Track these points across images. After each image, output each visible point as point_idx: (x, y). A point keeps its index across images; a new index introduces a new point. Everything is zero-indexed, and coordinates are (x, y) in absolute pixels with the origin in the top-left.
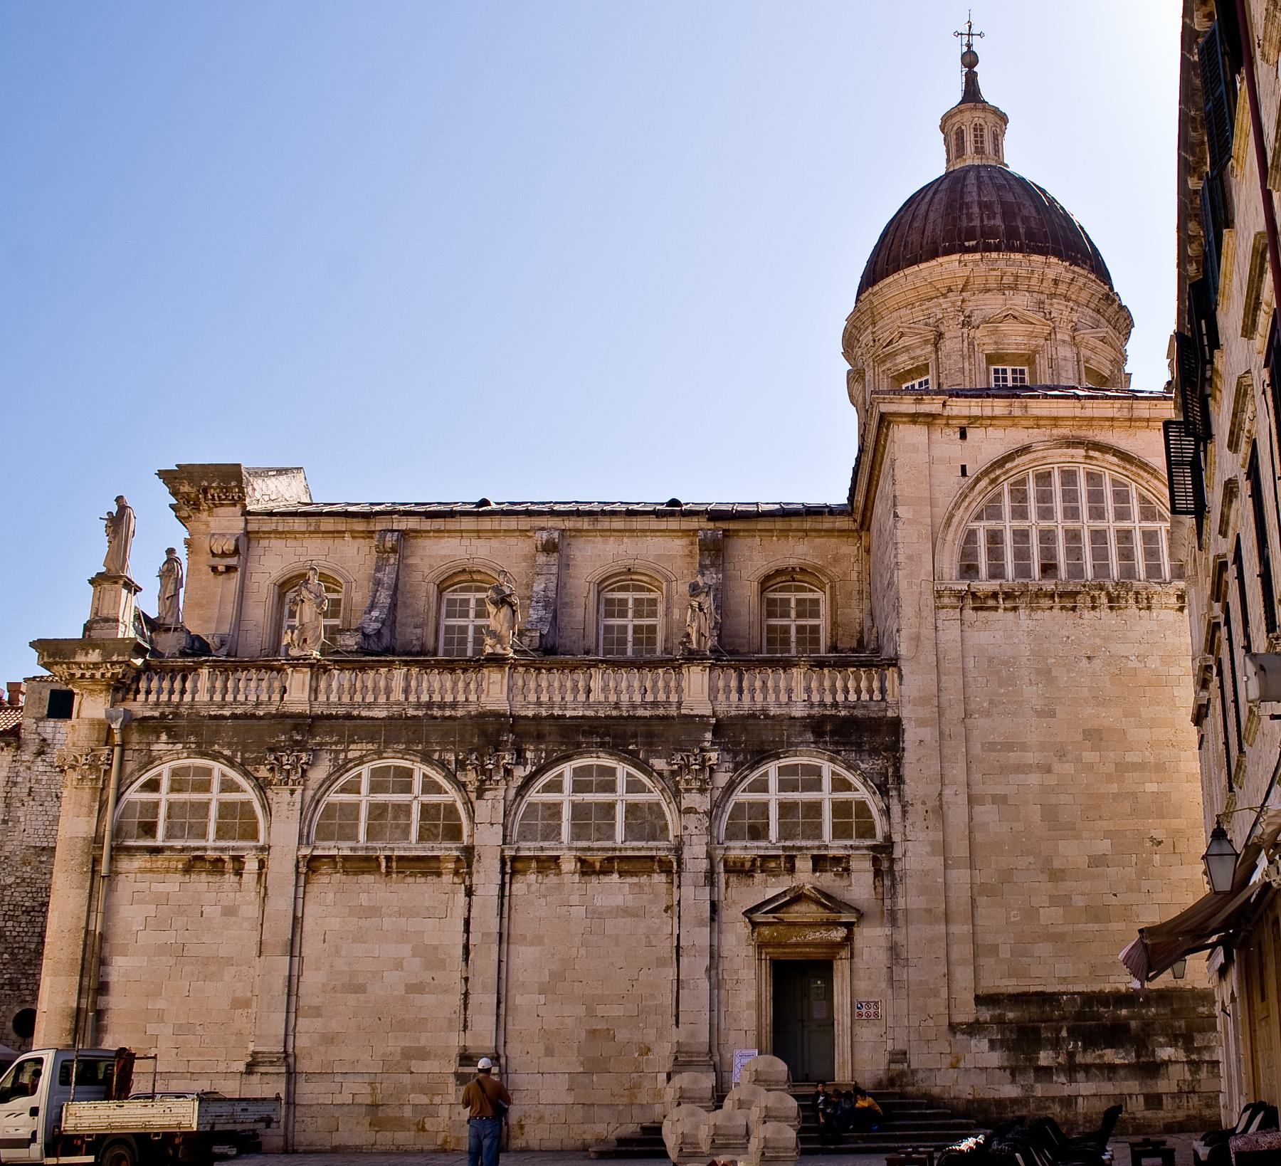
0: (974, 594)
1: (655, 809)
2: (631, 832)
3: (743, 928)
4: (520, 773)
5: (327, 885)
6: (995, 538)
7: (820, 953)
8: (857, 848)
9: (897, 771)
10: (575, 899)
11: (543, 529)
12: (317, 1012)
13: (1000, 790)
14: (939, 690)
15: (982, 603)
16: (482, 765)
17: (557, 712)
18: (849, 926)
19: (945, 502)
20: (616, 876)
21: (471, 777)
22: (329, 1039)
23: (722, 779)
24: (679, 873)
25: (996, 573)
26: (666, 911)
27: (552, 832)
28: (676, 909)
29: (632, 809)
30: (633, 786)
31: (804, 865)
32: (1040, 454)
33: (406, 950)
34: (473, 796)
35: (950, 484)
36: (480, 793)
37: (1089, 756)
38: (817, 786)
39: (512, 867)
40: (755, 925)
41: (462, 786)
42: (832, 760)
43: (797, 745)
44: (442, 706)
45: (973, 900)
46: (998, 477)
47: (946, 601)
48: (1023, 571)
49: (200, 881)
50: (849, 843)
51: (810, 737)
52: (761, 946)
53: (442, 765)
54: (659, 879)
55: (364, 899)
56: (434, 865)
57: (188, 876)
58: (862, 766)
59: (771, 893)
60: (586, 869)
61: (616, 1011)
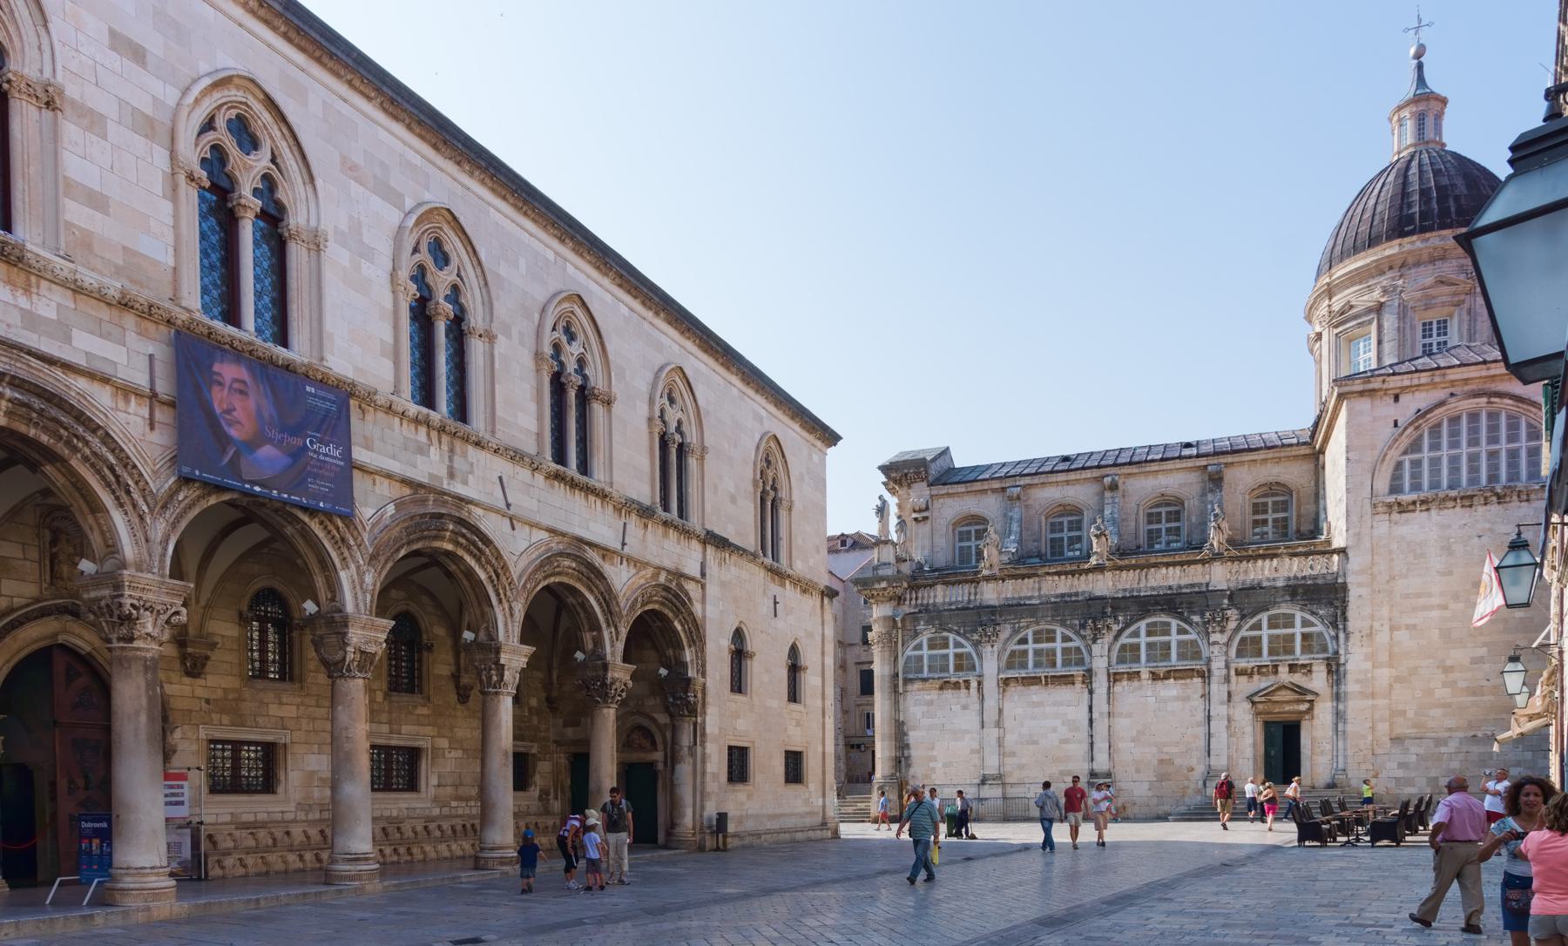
0: (1399, 504)
1: (1194, 643)
2: (1181, 656)
3: (1248, 706)
4: (1116, 628)
5: (1015, 691)
7: (1293, 717)
8: (1317, 659)
9: (1344, 613)
10: (1149, 693)
11: (1108, 476)
12: (1013, 754)
13: (1412, 621)
14: (1373, 564)
15: (1403, 508)
16: (1095, 625)
17: (1135, 594)
18: (1311, 702)
20: (1172, 680)
21: (1088, 632)
22: (1021, 767)
23: (1232, 625)
24: (1209, 677)
26: (1202, 696)
27: (1137, 659)
30: (1181, 631)
31: (1283, 670)
32: (1453, 405)
33: (1058, 723)
34: (1090, 642)
36: (1094, 641)
39: (1114, 678)
40: (1253, 703)
41: (1084, 637)
42: (1302, 610)
43: (1279, 603)
44: (1070, 595)
45: (1391, 686)
46: (1420, 425)
47: (1380, 509)
48: (1435, 485)
50: (1313, 656)
51: (1288, 598)
52: (1258, 714)
53: (1072, 627)
54: (1200, 680)
55: (1035, 698)
56: (1071, 679)
58: (1321, 612)
59: (1263, 685)
60: (1155, 677)
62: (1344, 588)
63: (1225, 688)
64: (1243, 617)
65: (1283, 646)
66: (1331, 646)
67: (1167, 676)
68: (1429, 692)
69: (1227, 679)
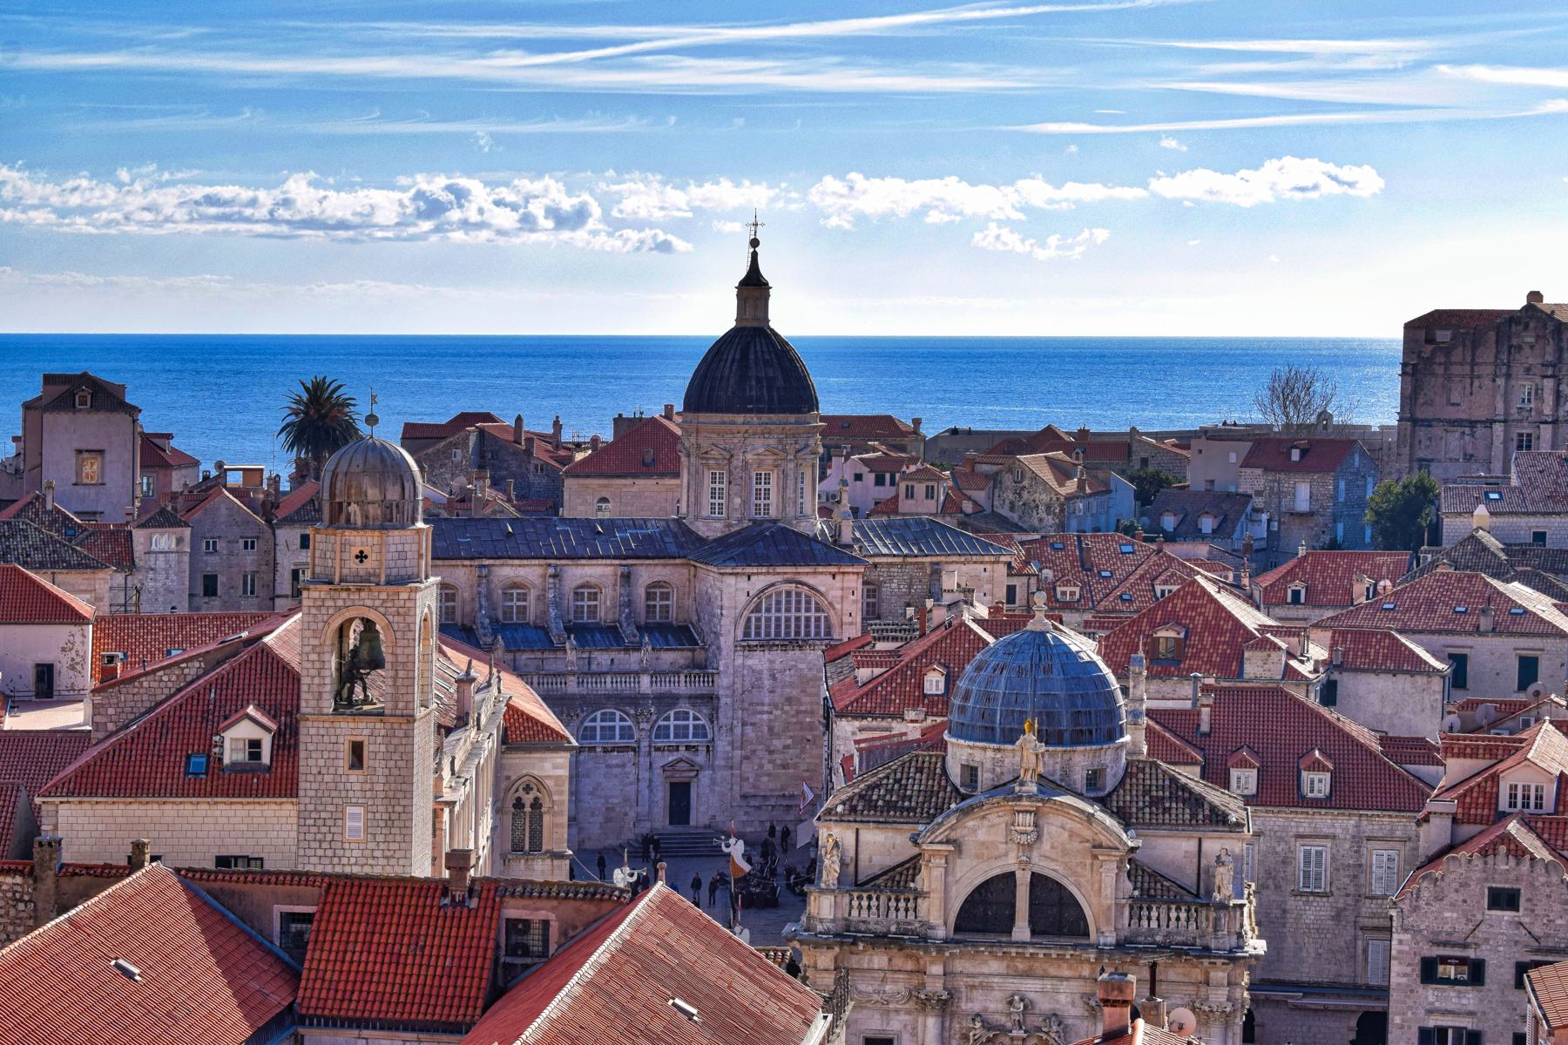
3: (660, 771)
4: (582, 715)
6: (758, 620)
7: (686, 780)
15: (750, 648)
19: (740, 606)
23: (654, 717)
25: (758, 634)
27: (594, 737)
29: (622, 728)
30: (622, 719)
31: (682, 749)
35: (743, 599)
37: (786, 708)
38: (688, 719)
59: (670, 759)
60: (605, 750)
61: (616, 801)
62: (718, 698)
63: (647, 759)
64: (659, 713)
65: (681, 732)
66: (710, 736)
67: (613, 750)
68: (761, 766)
69: (650, 754)
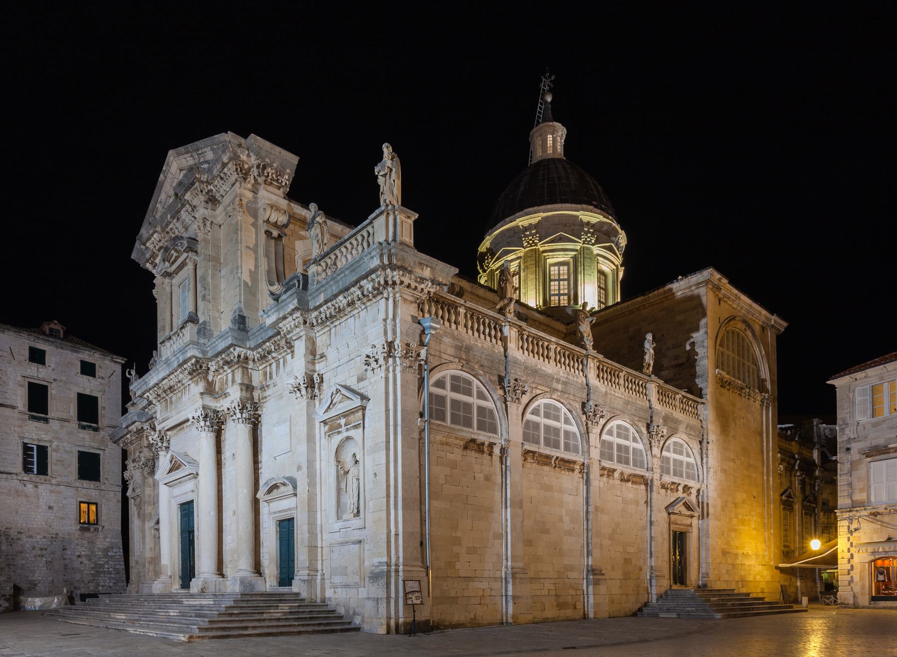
20: (630, 483)
28: (649, 503)
49: (472, 455)
54: (643, 487)
57: (465, 452)
